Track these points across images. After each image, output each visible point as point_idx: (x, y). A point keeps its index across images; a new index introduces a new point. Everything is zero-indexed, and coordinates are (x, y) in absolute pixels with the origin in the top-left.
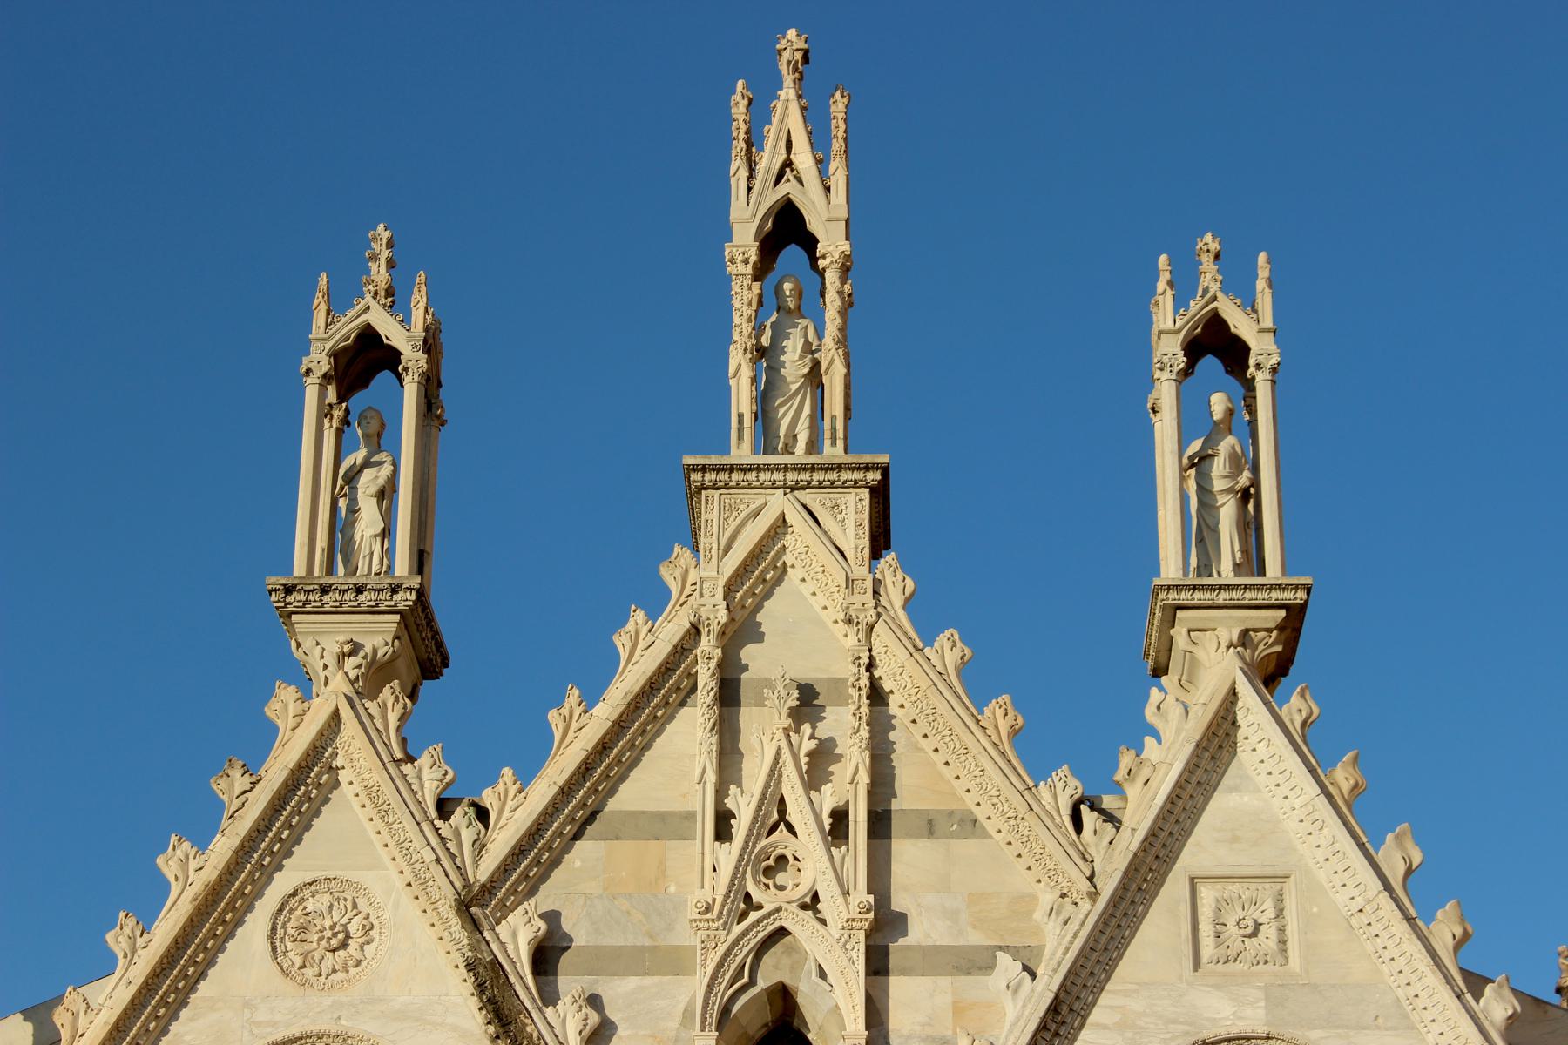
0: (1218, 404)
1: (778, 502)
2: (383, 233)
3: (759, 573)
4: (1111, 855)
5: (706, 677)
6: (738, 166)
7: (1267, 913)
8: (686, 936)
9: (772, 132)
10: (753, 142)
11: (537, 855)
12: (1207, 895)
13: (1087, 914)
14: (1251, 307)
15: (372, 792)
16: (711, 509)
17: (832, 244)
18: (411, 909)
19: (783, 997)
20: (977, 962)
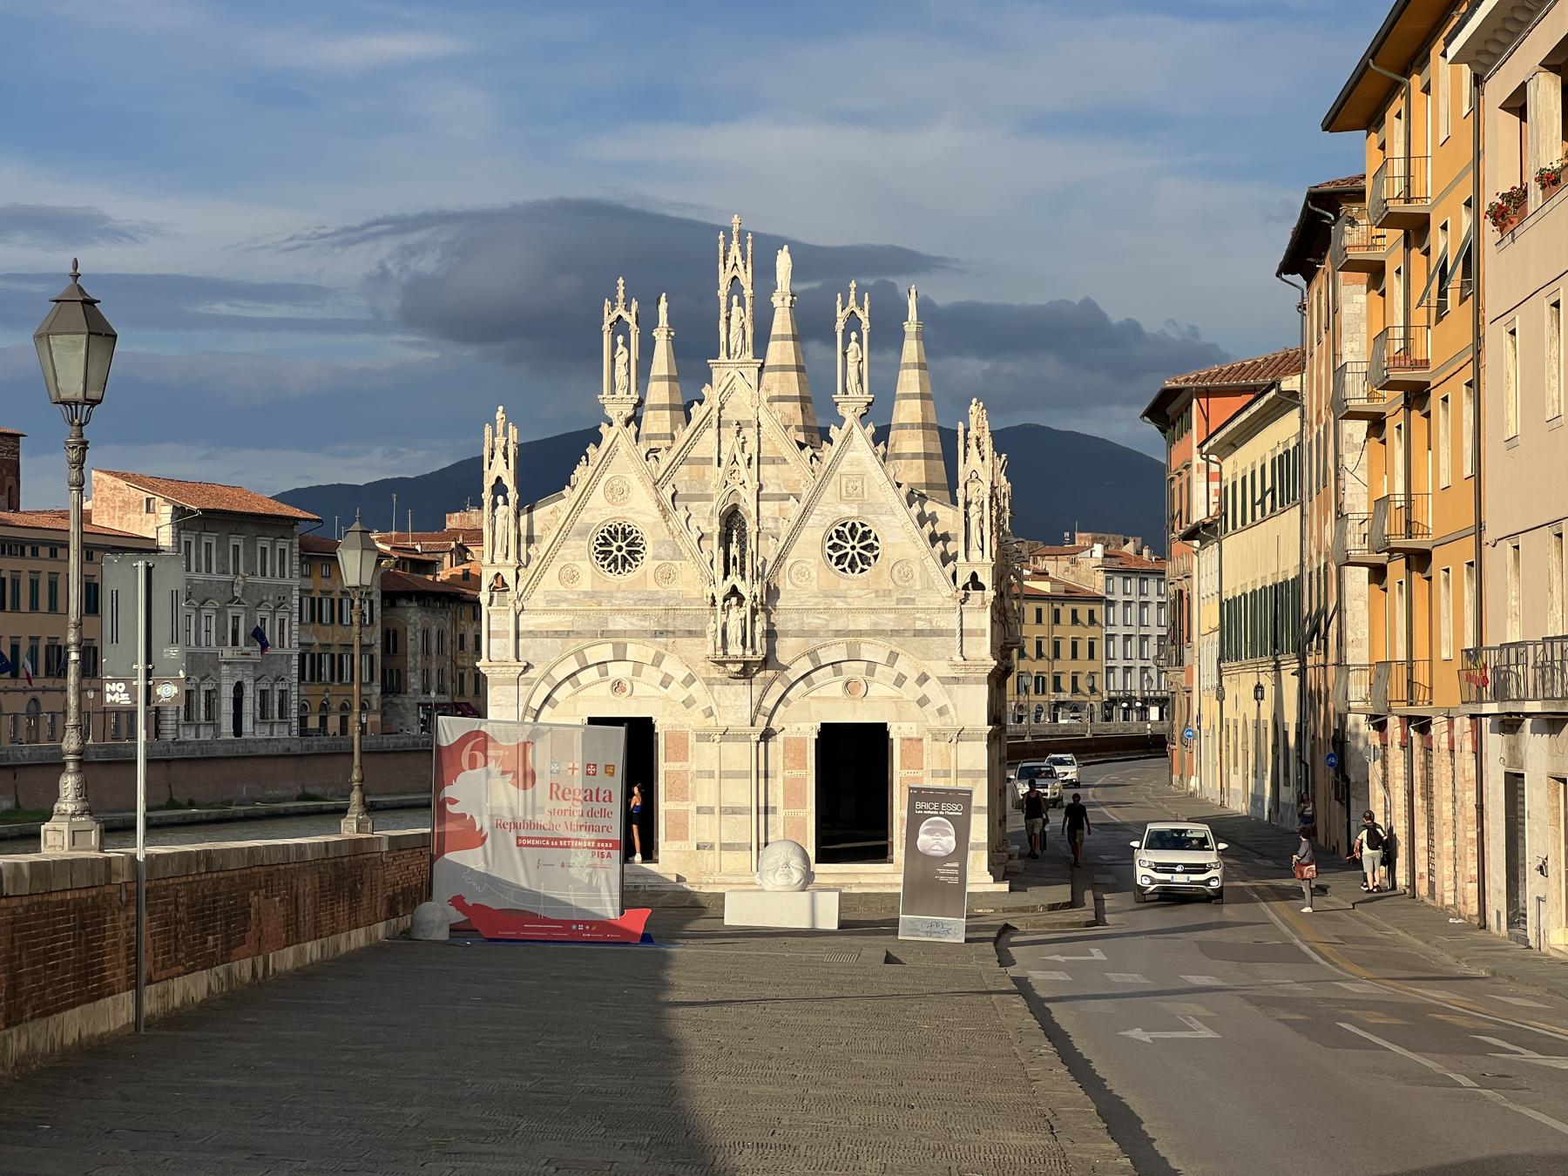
0: (854, 335)
1: (734, 372)
2: (621, 281)
3: (729, 390)
4: (820, 469)
5: (715, 424)
6: (721, 266)
7: (859, 484)
8: (711, 490)
9: (731, 256)
10: (725, 259)
11: (671, 469)
12: (844, 480)
13: (814, 485)
14: (862, 309)
15: (628, 454)
16: (716, 374)
17: (748, 292)
18: (640, 485)
19: (735, 506)
20: (785, 498)
